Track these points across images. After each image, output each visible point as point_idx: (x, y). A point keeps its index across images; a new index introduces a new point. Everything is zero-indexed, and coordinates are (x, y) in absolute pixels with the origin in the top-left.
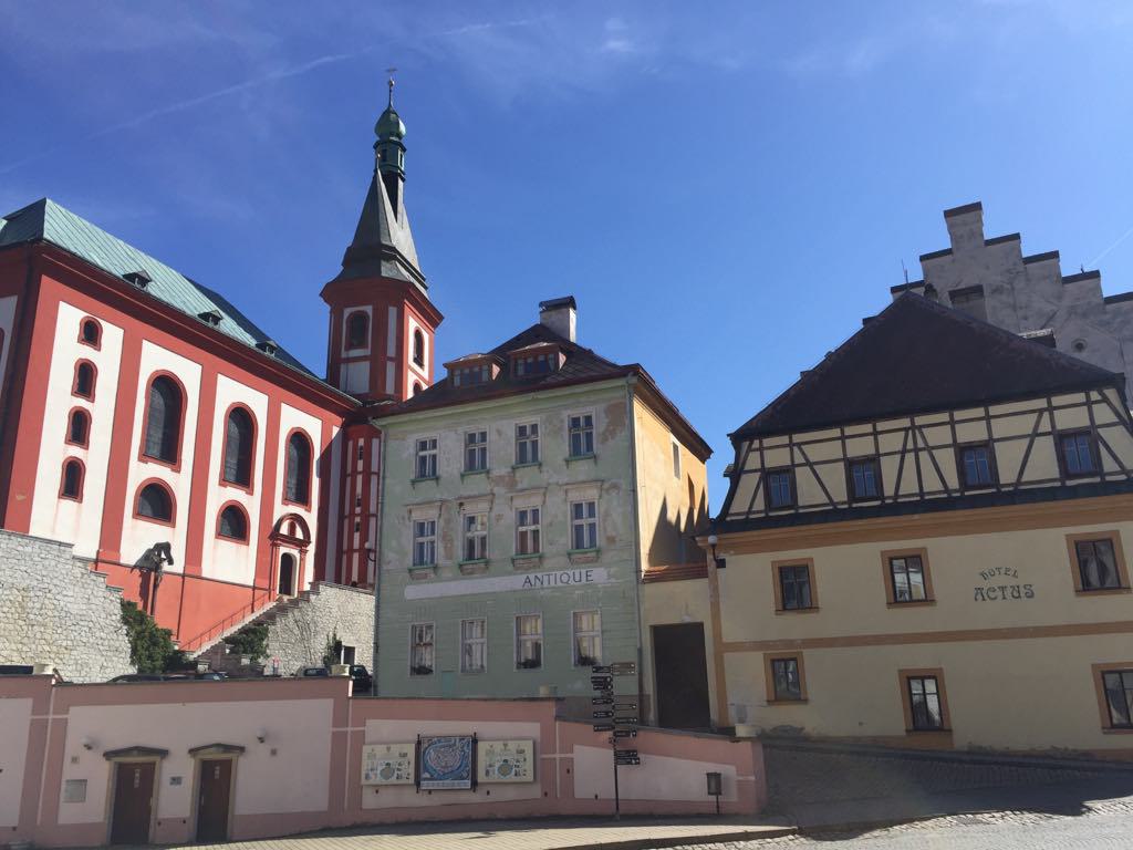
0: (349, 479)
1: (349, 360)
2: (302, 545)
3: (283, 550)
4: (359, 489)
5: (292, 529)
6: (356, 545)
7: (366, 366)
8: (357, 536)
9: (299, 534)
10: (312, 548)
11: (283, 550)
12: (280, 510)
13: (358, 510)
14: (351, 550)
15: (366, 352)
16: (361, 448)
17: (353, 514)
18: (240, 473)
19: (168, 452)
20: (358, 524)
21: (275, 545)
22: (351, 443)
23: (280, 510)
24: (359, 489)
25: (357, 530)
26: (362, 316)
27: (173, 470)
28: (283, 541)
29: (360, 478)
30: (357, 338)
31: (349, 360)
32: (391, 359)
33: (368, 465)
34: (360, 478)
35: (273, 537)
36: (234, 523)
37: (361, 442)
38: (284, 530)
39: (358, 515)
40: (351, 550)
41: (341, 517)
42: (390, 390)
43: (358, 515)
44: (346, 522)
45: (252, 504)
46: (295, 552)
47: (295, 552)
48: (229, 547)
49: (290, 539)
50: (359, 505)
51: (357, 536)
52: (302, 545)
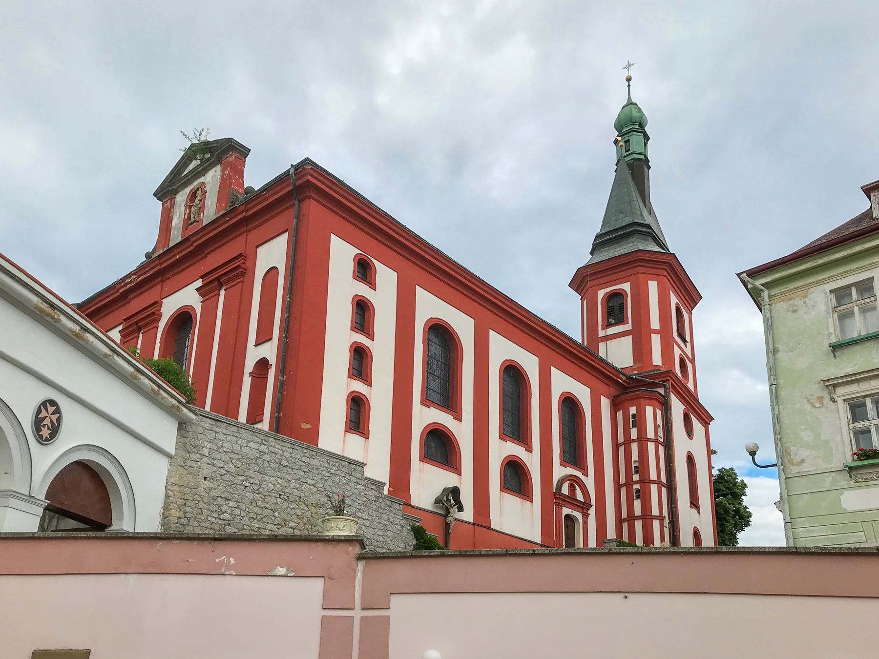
0: (621, 450)
1: (607, 338)
2: (584, 507)
3: (566, 511)
4: (635, 456)
5: (572, 487)
6: (638, 511)
7: (629, 339)
8: (637, 504)
9: (580, 496)
10: (592, 511)
11: (566, 511)
12: (559, 471)
13: (636, 477)
14: (631, 518)
15: (628, 327)
16: (634, 416)
17: (629, 483)
18: (516, 428)
19: (446, 396)
20: (638, 491)
21: (559, 506)
22: (620, 414)
23: (559, 471)
24: (635, 456)
25: (638, 497)
26: (618, 295)
27: (454, 418)
28: (564, 500)
29: (634, 447)
30: (615, 310)
31: (607, 338)
32: (656, 332)
33: (642, 431)
34: (634, 447)
35: (554, 499)
36: (516, 477)
37: (633, 410)
38: (565, 490)
39: (636, 482)
40: (631, 518)
41: (618, 487)
42: (657, 359)
43: (636, 482)
44: (623, 491)
45: (532, 462)
46: (578, 515)
47: (578, 515)
48: (512, 501)
49: (571, 501)
50: (636, 472)
51: (637, 504)
52: (584, 507)
